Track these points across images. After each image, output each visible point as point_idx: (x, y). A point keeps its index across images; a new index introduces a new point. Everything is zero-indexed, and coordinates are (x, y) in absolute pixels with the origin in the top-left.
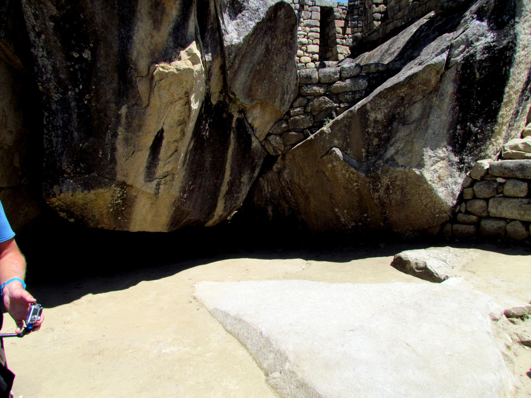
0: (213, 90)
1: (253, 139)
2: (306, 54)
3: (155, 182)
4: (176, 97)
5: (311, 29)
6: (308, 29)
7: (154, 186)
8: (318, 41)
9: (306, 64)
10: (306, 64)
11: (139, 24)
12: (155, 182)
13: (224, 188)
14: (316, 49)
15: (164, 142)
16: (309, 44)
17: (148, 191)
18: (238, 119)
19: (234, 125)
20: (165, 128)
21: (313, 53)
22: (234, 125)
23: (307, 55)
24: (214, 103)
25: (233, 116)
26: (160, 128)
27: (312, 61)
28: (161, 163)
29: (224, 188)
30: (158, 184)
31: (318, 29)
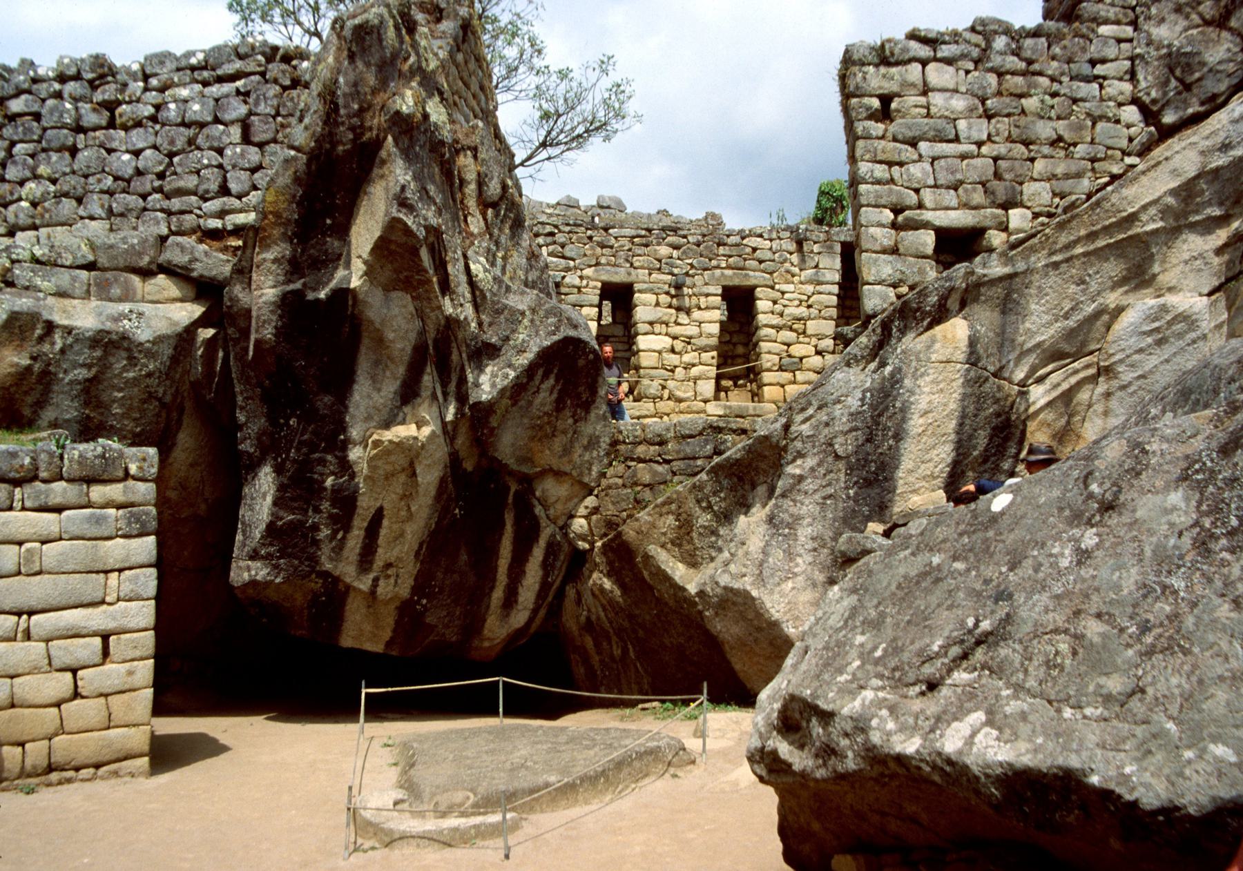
0: (462, 454)
1: (544, 522)
2: (801, 339)
3: (371, 576)
4: (399, 468)
5: (818, 288)
6: (810, 289)
7: (370, 582)
8: (834, 312)
9: (801, 359)
10: (801, 359)
11: (356, 387)
12: (371, 576)
13: (498, 594)
14: (829, 327)
15: (385, 522)
16: (809, 319)
17: (362, 587)
18: (516, 492)
19: (510, 499)
20: (385, 506)
21: (821, 337)
22: (510, 499)
23: (807, 340)
24: (470, 469)
25: (509, 489)
26: (378, 505)
27: (818, 353)
28: (380, 550)
29: (498, 594)
30: (376, 580)
31: (835, 289)
